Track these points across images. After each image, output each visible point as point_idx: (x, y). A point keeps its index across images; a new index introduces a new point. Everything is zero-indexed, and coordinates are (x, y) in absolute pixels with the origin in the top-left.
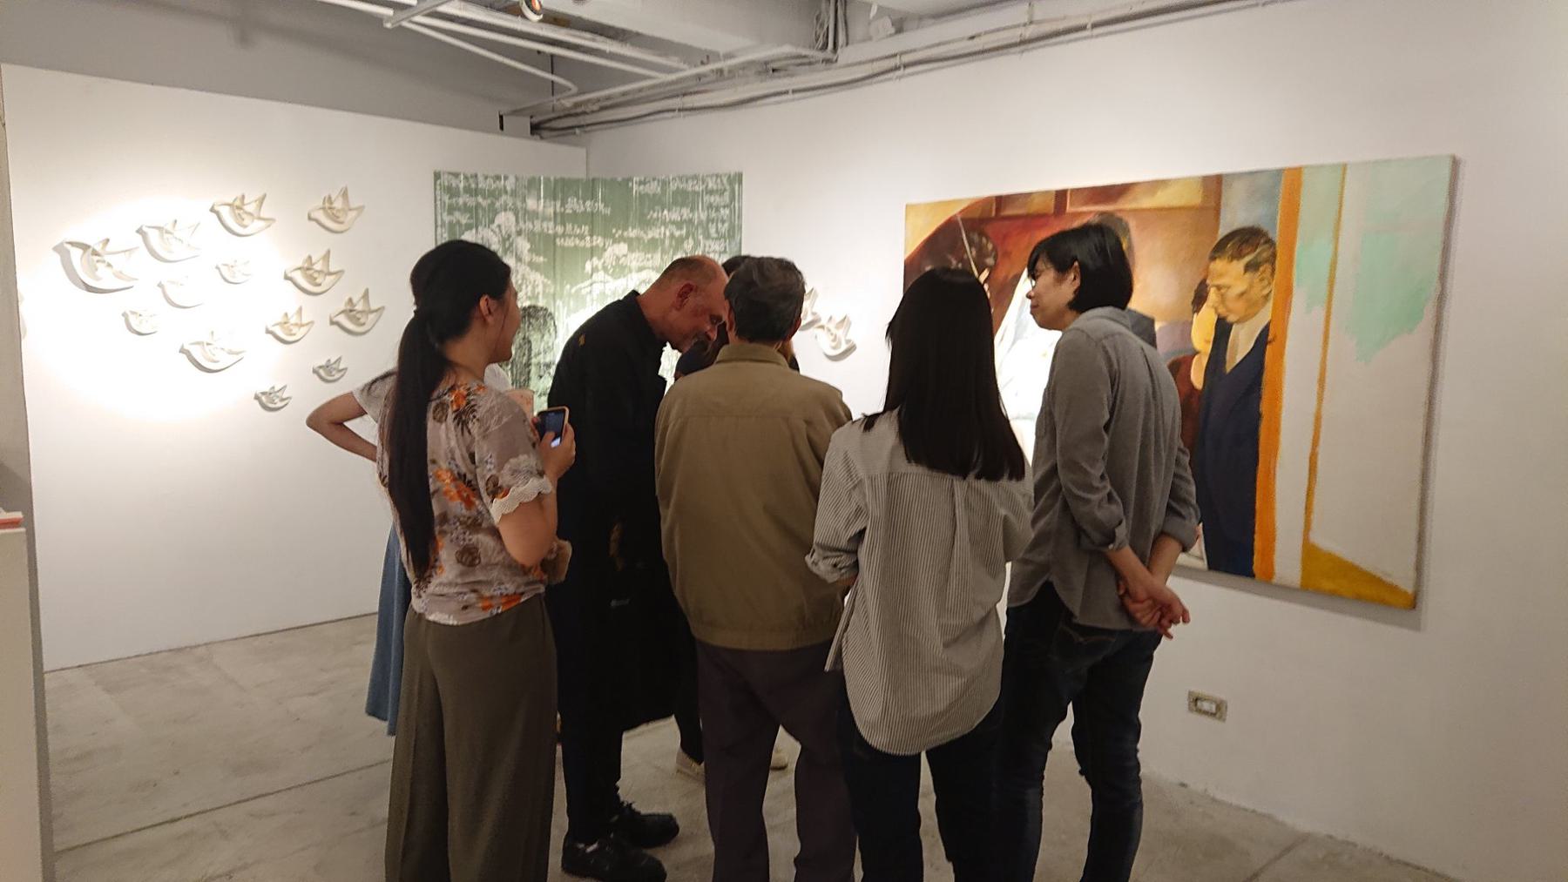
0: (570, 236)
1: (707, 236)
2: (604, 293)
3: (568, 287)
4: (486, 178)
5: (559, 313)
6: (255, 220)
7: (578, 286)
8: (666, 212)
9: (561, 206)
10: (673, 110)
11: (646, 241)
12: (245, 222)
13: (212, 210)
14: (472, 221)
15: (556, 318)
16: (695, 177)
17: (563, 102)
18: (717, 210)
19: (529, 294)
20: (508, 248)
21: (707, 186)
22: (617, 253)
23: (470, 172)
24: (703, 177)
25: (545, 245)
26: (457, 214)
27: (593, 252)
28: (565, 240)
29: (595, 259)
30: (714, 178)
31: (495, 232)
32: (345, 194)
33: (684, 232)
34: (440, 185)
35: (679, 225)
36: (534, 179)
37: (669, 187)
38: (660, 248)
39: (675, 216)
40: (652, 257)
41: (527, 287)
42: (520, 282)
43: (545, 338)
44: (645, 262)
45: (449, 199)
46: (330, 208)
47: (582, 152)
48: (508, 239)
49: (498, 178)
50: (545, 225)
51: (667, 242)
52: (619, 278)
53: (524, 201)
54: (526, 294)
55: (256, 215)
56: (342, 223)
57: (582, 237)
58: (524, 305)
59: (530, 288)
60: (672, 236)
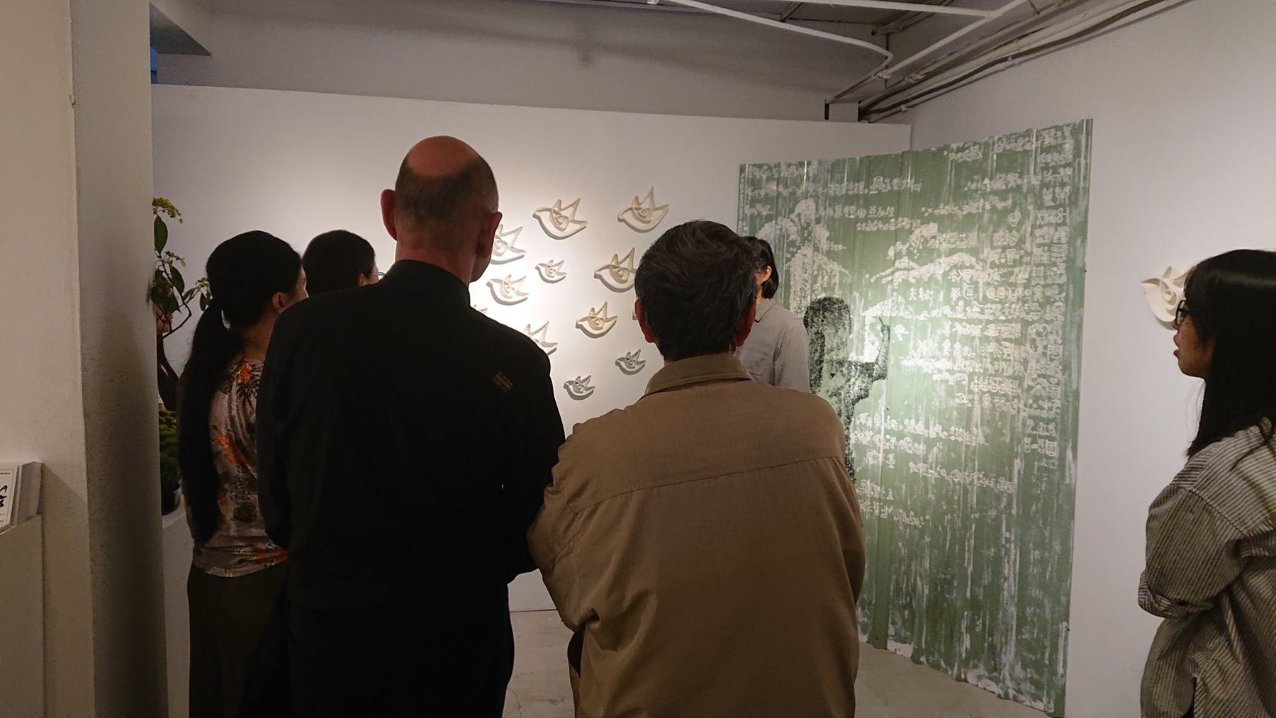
0: (873, 220)
1: (1040, 206)
2: (908, 281)
3: (867, 276)
4: (789, 166)
5: (855, 305)
6: (570, 224)
7: (878, 276)
8: (987, 181)
9: (865, 188)
10: (1005, 59)
11: (961, 217)
12: (562, 226)
13: (535, 216)
14: (772, 212)
15: (851, 312)
16: (1028, 133)
17: (880, 74)
18: (1055, 171)
19: (825, 286)
20: (806, 239)
21: (1043, 142)
22: (925, 234)
23: (772, 162)
24: (1038, 132)
25: (844, 231)
26: (758, 206)
27: (900, 235)
28: (867, 226)
29: (899, 243)
30: (1053, 131)
31: (794, 222)
32: (651, 194)
33: (1009, 202)
34: (744, 178)
35: (1002, 195)
36: (838, 161)
37: (993, 150)
38: (977, 227)
39: (999, 185)
40: (967, 237)
41: (823, 277)
42: (816, 273)
43: (839, 333)
44: (958, 243)
45: (752, 191)
46: (636, 209)
47: (906, 128)
48: (807, 228)
49: (801, 164)
50: (846, 210)
51: (986, 217)
52: (927, 264)
53: (826, 185)
54: (822, 285)
55: (570, 219)
56: (648, 222)
57: (886, 220)
58: (819, 297)
59: (826, 278)
60: (994, 208)
